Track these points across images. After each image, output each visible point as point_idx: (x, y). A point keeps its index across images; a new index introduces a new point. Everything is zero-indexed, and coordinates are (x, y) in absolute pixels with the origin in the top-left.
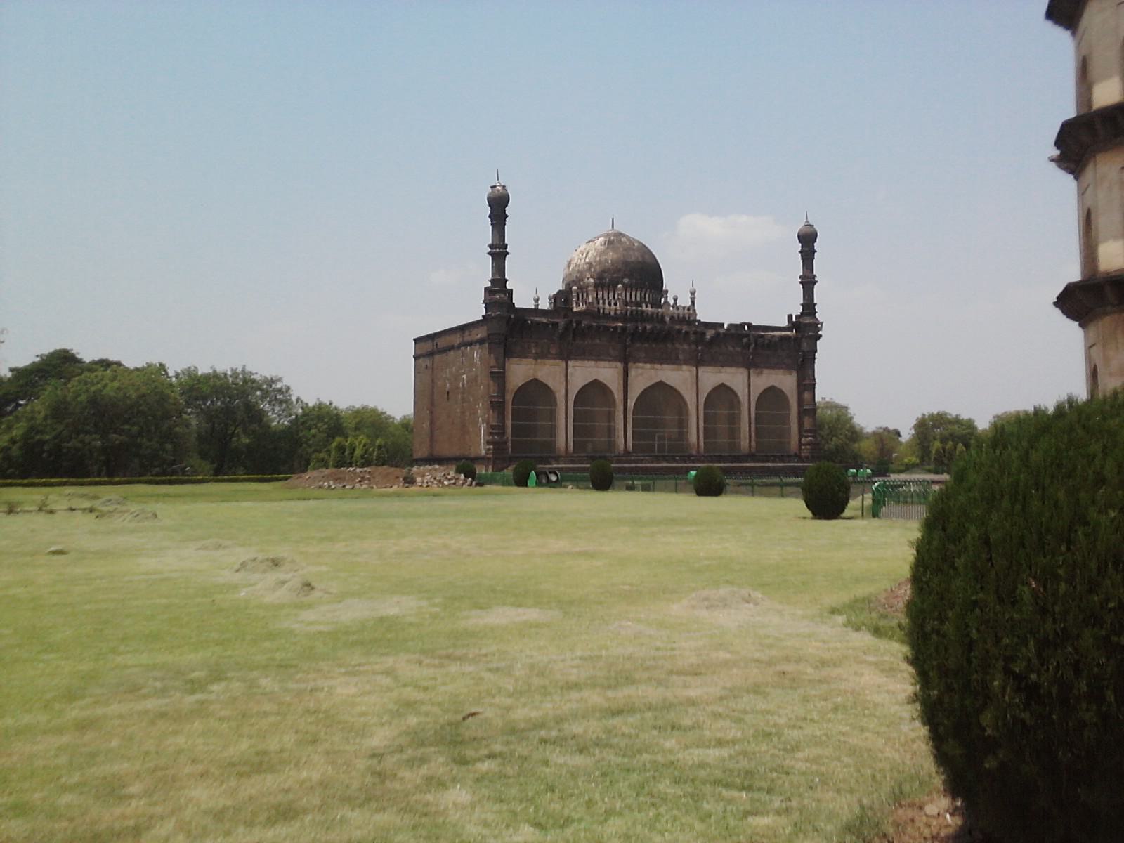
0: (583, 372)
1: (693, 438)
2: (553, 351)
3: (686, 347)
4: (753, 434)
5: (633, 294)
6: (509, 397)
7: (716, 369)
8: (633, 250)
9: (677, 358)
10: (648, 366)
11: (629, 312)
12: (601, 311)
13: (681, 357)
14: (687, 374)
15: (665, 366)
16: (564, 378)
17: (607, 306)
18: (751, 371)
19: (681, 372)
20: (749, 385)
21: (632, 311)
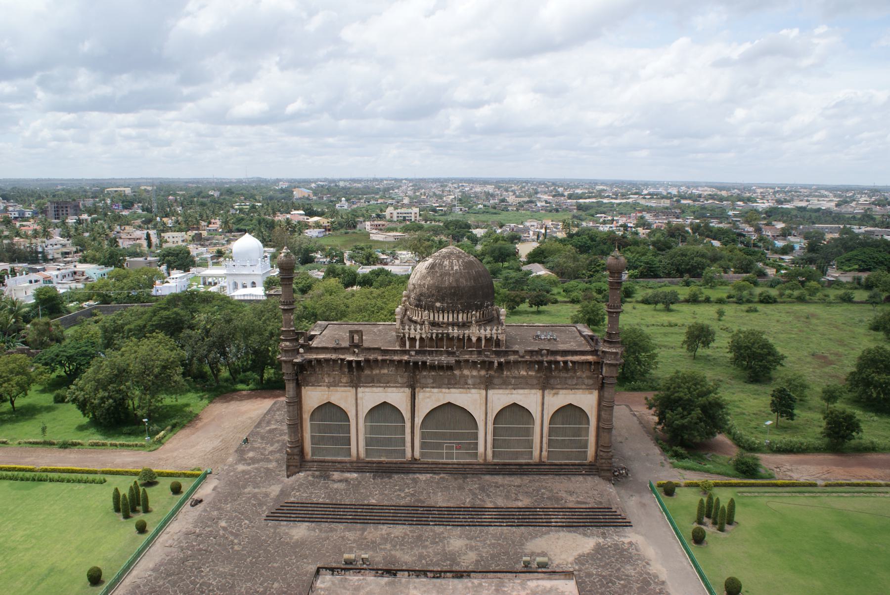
0: (371, 397)
1: (481, 449)
2: (344, 380)
3: (475, 373)
4: (545, 446)
5: (446, 316)
6: (306, 416)
7: (507, 391)
8: (450, 275)
9: (467, 384)
10: (436, 390)
11: (434, 336)
12: (407, 336)
13: (470, 382)
14: (477, 396)
15: (453, 390)
16: (354, 402)
17: (412, 331)
18: (546, 392)
19: (469, 395)
20: (543, 404)
21: (437, 334)
